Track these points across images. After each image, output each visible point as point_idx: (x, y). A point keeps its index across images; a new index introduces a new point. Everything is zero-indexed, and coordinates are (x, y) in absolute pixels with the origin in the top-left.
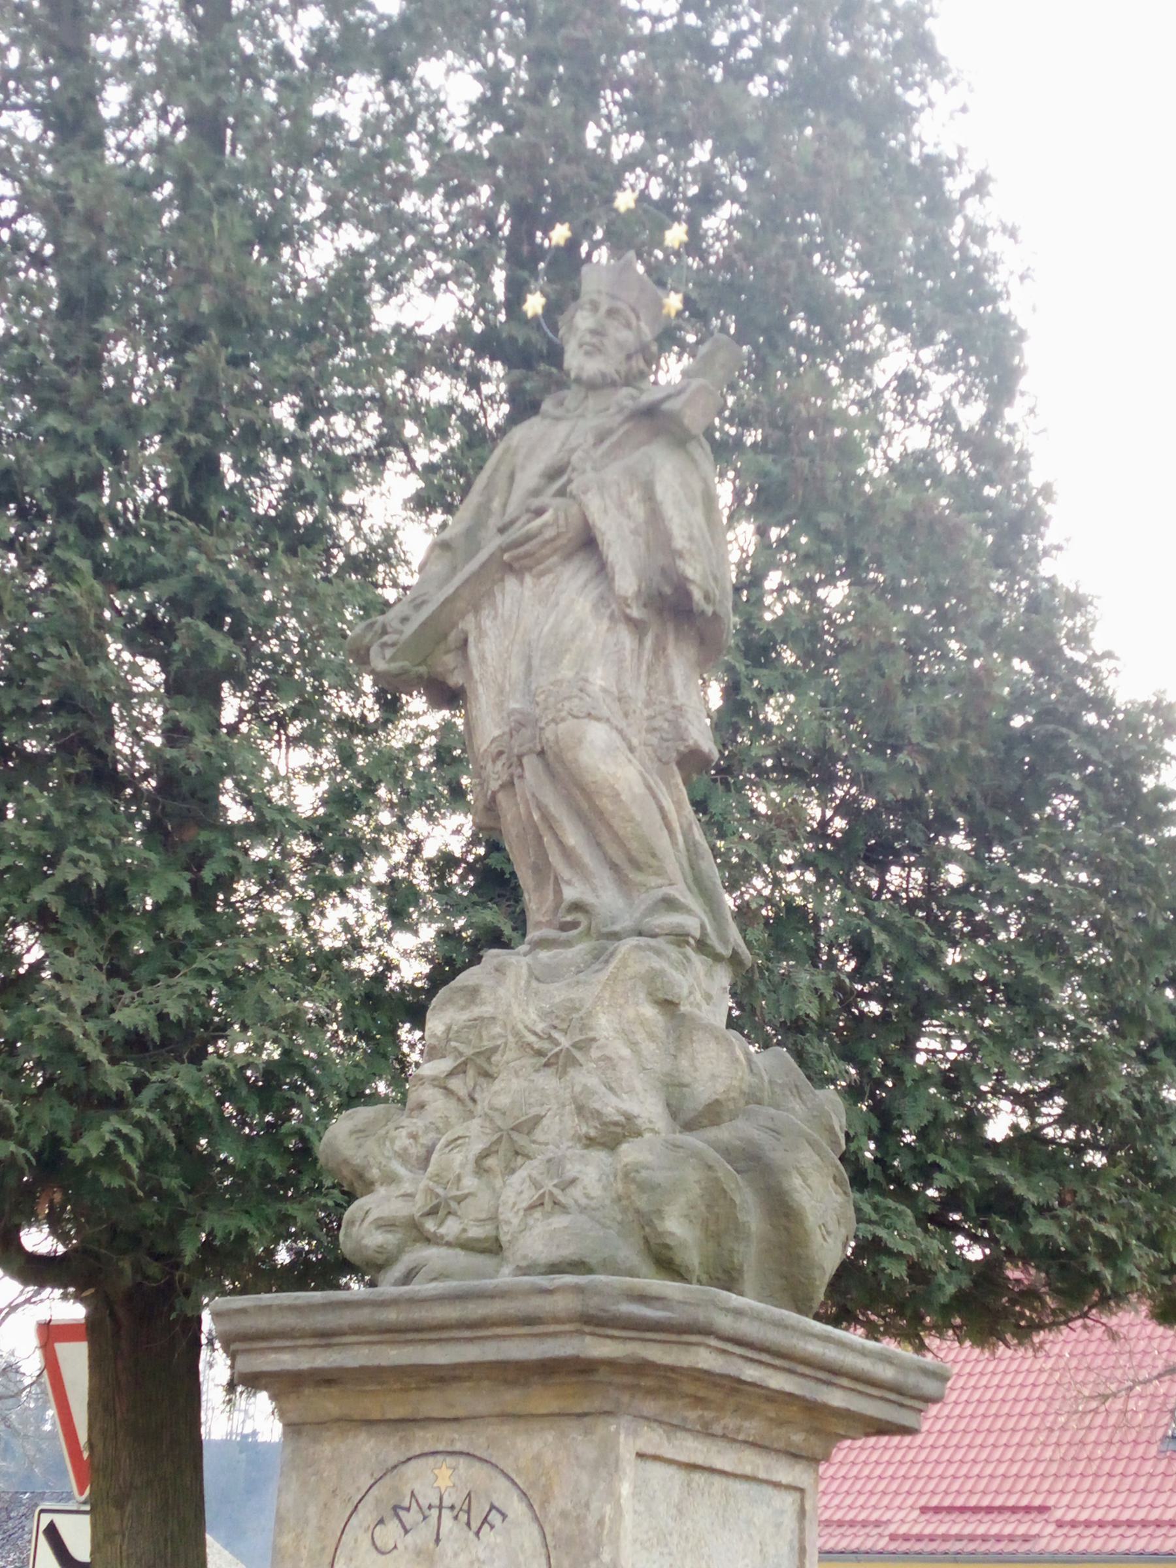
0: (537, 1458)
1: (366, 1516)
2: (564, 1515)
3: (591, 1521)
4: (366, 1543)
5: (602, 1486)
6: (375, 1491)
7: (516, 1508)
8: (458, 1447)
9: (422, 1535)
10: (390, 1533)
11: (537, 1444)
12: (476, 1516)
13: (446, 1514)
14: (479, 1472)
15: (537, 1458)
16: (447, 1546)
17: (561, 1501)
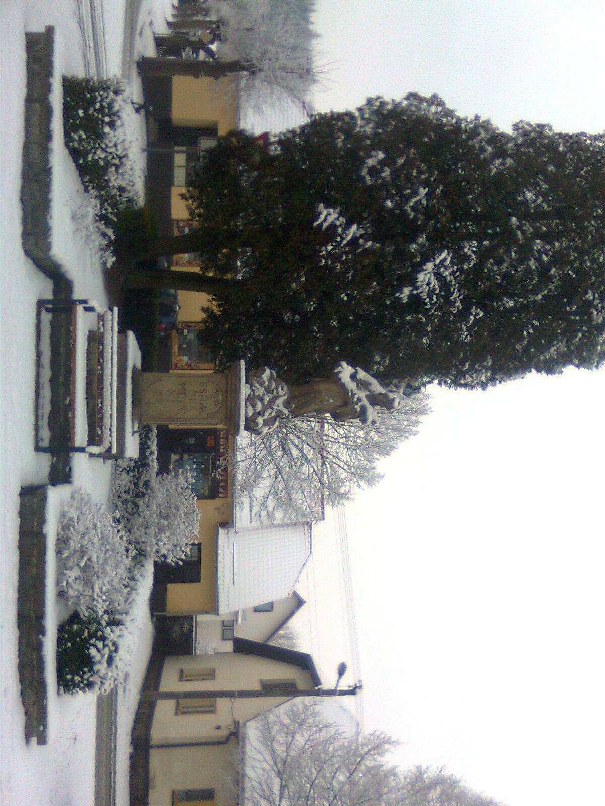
7: (217, 409)
10: (215, 391)
12: (216, 403)
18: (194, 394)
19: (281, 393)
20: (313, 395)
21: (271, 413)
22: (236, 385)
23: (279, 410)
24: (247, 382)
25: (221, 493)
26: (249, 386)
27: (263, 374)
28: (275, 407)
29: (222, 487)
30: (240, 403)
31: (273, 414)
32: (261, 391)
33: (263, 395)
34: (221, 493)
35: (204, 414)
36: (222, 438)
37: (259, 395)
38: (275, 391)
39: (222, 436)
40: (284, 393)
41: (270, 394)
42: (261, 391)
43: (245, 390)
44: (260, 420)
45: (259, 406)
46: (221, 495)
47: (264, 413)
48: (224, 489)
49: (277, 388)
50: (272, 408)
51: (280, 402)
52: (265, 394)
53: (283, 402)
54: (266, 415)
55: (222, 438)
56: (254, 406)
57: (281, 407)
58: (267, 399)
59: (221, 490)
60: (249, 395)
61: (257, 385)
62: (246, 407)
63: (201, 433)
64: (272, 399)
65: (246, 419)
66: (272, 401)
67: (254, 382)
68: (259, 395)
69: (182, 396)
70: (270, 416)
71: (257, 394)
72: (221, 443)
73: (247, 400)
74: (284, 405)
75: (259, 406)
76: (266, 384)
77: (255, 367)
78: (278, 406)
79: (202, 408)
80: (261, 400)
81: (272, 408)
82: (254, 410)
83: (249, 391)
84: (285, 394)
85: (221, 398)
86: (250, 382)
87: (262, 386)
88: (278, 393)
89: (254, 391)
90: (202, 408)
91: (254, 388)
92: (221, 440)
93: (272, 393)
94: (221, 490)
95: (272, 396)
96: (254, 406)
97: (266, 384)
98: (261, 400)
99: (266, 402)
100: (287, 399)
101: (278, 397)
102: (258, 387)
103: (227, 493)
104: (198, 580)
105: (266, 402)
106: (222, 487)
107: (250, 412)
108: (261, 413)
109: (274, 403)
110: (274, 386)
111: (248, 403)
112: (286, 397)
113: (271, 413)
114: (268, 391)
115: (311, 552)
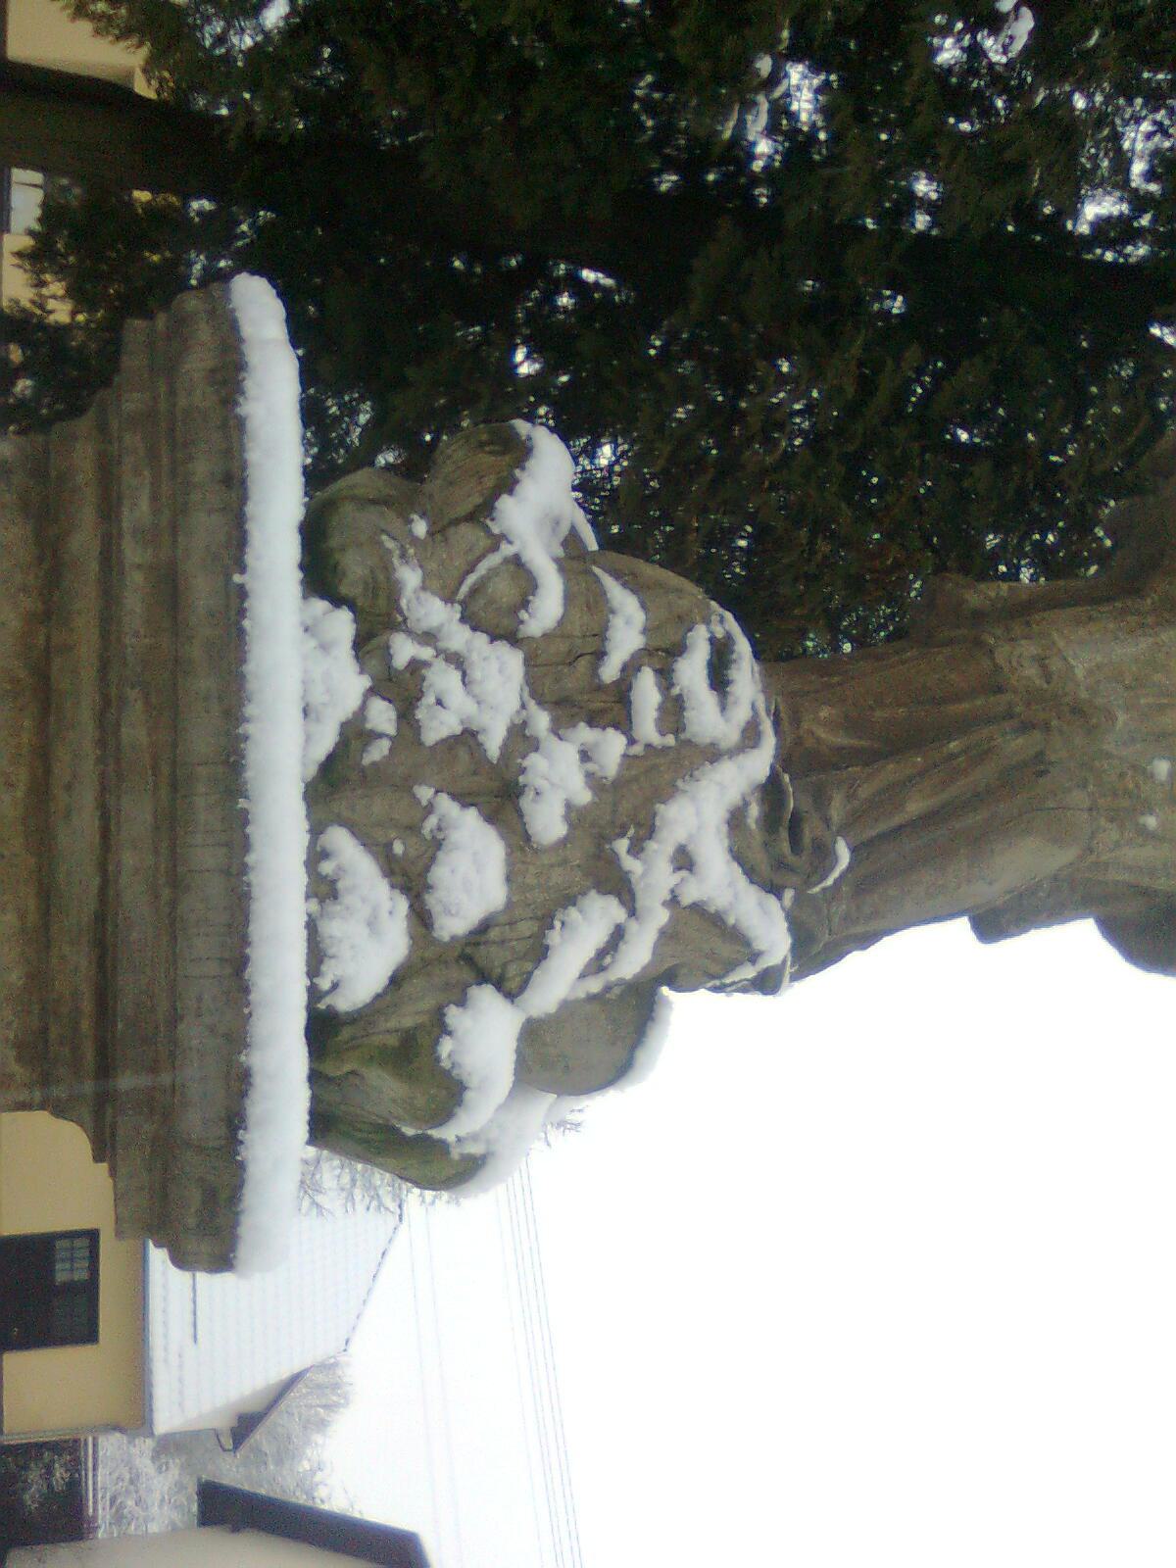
19: (708, 719)
20: (1016, 746)
21: (618, 937)
22: (169, 588)
23: (697, 908)
24: (320, 575)
26: (342, 625)
27: (508, 485)
28: (654, 875)
30: (236, 834)
31: (635, 959)
32: (484, 691)
33: (520, 738)
37: (468, 737)
38: (647, 693)
40: (741, 714)
41: (593, 721)
42: (484, 691)
43: (299, 675)
44: (485, 1035)
45: (474, 876)
47: (540, 953)
49: (663, 655)
50: (622, 889)
51: (702, 814)
52: (541, 721)
53: (735, 819)
54: (559, 981)
56: (412, 879)
57: (720, 882)
58: (560, 779)
60: (355, 733)
61: (435, 612)
62: (324, 889)
64: (619, 785)
65: (324, 1029)
66: (625, 810)
67: (410, 577)
68: (468, 737)
70: (595, 985)
71: (438, 726)
73: (333, 784)
74: (737, 856)
75: (474, 876)
76: (548, 608)
77: (408, 396)
78: (684, 861)
80: (500, 796)
81: (622, 889)
82: (421, 918)
83: (348, 685)
84: (751, 736)
86: (354, 567)
87: (513, 639)
88: (674, 710)
89: (402, 689)
91: (404, 650)
93: (611, 707)
95: (612, 746)
96: (412, 879)
97: (548, 608)
98: (500, 796)
99: (548, 822)
100: (771, 790)
101: (680, 759)
102: (459, 637)
104: (87, 1333)
105: (548, 822)
107: (370, 956)
108: (492, 959)
109: (645, 830)
110: (628, 628)
111: (340, 840)
112: (760, 763)
113: (618, 937)
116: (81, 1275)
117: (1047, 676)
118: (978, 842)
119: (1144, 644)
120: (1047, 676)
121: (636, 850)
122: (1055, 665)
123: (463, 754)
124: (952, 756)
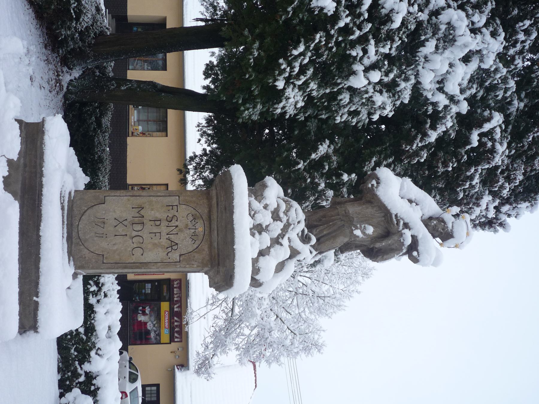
0: (204, 250)
1: (194, 212)
2: (194, 257)
3: (193, 263)
4: (189, 213)
5: (200, 265)
6: (198, 214)
8: (206, 232)
9: (190, 226)
10: (191, 218)
11: (206, 249)
13: (193, 231)
14: (201, 237)
15: (204, 250)
16: (188, 231)
17: (197, 255)
18: (158, 223)
25: (177, 338)
29: (177, 332)
34: (177, 338)
35: (175, 256)
36: (176, 288)
39: (175, 286)
46: (176, 340)
48: (179, 334)
55: (176, 288)
59: (176, 335)
63: (156, 284)
69: (139, 227)
72: (175, 292)
79: (173, 245)
85: (200, 229)
90: (173, 245)
92: (175, 290)
94: (176, 335)
103: (181, 338)
106: (177, 332)
114: (276, 216)
115: (256, 386)
116: (154, 399)
117: (346, 213)
118: (334, 237)
119: (361, 208)
120: (346, 213)
121: (282, 238)
122: (347, 211)
123: (259, 227)
124: (331, 225)
